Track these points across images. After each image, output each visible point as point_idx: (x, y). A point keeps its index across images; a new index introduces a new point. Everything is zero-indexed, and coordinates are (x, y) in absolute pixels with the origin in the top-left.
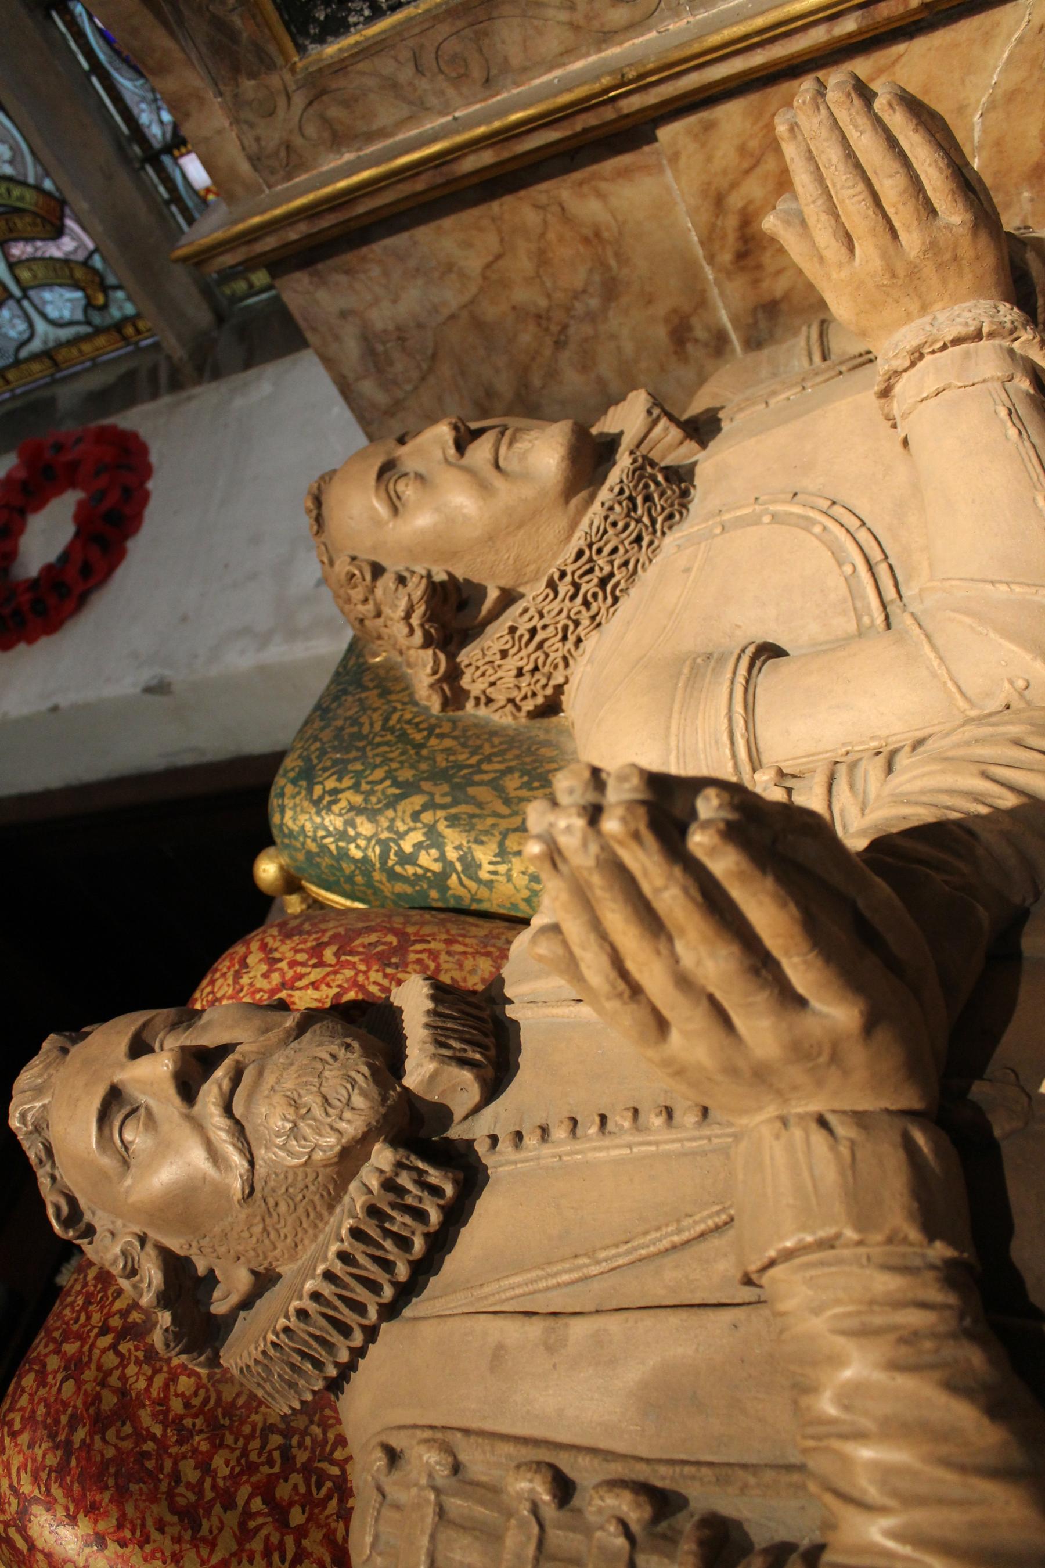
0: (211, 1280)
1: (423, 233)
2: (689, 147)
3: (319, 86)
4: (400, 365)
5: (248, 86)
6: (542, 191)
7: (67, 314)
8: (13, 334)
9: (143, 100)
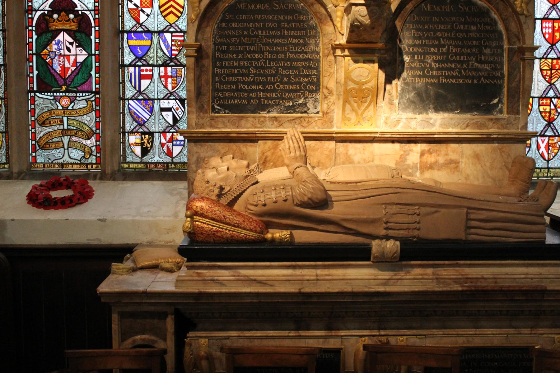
0: (224, 189)
1: (217, 144)
2: (262, 145)
3: (212, 118)
5: (202, 114)
6: (238, 144)
7: (75, 157)
8: (56, 156)
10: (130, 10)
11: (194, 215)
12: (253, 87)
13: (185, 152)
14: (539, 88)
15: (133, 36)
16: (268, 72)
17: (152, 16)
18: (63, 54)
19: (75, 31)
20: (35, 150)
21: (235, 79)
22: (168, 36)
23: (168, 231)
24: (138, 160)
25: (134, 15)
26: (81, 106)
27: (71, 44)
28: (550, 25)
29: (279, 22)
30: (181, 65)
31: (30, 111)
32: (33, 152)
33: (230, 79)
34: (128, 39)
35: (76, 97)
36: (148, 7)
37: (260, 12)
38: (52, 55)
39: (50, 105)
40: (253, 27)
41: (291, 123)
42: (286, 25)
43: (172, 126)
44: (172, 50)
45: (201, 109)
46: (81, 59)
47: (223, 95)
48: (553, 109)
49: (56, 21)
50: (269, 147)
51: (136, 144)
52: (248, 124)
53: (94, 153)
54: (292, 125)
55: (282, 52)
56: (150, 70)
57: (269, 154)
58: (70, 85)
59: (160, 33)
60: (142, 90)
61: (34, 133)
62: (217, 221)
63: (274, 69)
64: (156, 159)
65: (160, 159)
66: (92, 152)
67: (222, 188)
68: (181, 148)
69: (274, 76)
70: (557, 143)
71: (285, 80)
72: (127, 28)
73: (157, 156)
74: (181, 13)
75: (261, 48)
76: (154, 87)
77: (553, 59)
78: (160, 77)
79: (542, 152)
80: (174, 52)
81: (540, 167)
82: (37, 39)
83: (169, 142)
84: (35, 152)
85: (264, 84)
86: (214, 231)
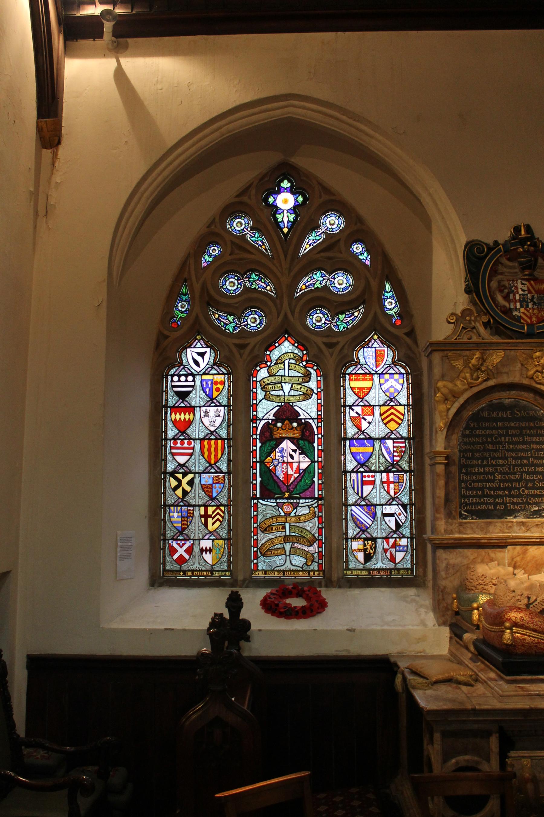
1: (466, 550)
3: (461, 524)
4: (451, 571)
5: (450, 520)
7: (297, 564)
8: (278, 563)
9: (352, 528)
10: (351, 418)
11: (514, 626)
12: (499, 493)
13: (409, 557)
15: (355, 443)
16: (512, 477)
17: (373, 424)
18: (286, 461)
19: (298, 439)
20: (256, 557)
21: (481, 485)
22: (389, 443)
23: (419, 640)
24: (361, 566)
25: (356, 423)
26: (304, 512)
27: (295, 451)
29: (521, 429)
30: (403, 471)
31: (253, 517)
32: (254, 559)
33: (476, 485)
34: (350, 446)
35: (299, 503)
36: (369, 415)
37: (502, 419)
38: (275, 462)
39: (272, 512)
40: (496, 434)
41: (539, 528)
42: (528, 432)
43: (395, 532)
44: (394, 456)
45: (449, 515)
46: (303, 466)
47: (469, 501)
49: (280, 429)
50: (518, 553)
51: (359, 550)
52: (496, 530)
53: (316, 560)
54: (540, 529)
55: (525, 458)
56: (372, 476)
57: (518, 559)
58: (292, 491)
59: (382, 439)
60: (364, 496)
61: (256, 540)
62: (539, 633)
63: (519, 475)
64: (379, 565)
65: (383, 565)
66: (314, 559)
67: (529, 598)
68: (403, 553)
69: (518, 481)
71: (530, 485)
72: (349, 435)
73: (380, 563)
74: (402, 420)
75: (505, 455)
76: (376, 492)
78: (383, 483)
80: (395, 458)
82: (260, 447)
83: (392, 547)
84: (257, 559)
85: (510, 489)
86: (536, 643)
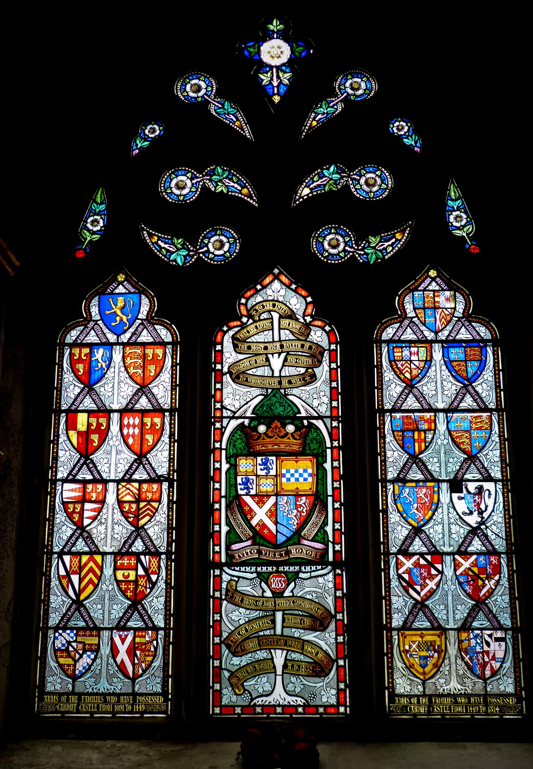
14: (116, 536)
28: (137, 421)
48: (141, 576)
70: (151, 642)
77: (141, 482)
79: (122, 661)
81: (118, 691)
